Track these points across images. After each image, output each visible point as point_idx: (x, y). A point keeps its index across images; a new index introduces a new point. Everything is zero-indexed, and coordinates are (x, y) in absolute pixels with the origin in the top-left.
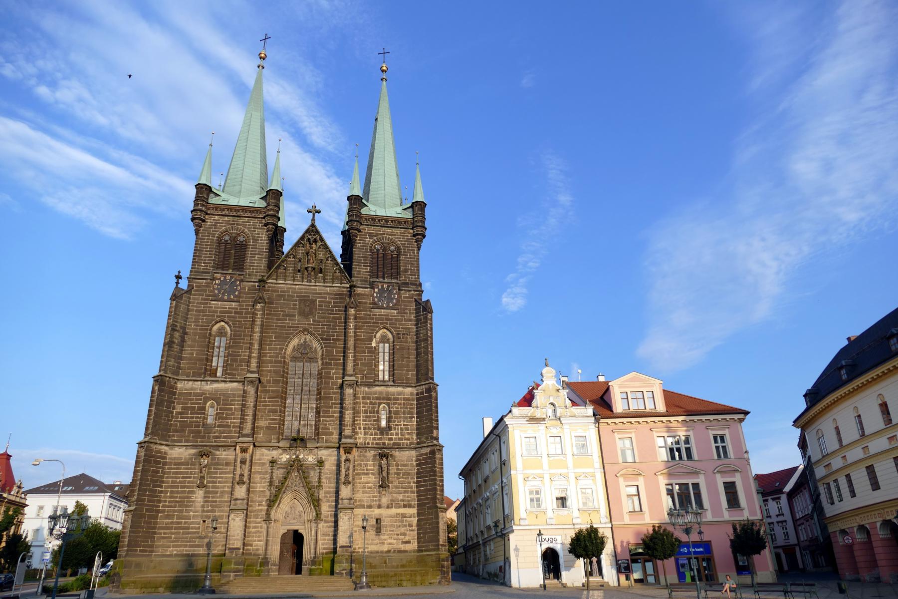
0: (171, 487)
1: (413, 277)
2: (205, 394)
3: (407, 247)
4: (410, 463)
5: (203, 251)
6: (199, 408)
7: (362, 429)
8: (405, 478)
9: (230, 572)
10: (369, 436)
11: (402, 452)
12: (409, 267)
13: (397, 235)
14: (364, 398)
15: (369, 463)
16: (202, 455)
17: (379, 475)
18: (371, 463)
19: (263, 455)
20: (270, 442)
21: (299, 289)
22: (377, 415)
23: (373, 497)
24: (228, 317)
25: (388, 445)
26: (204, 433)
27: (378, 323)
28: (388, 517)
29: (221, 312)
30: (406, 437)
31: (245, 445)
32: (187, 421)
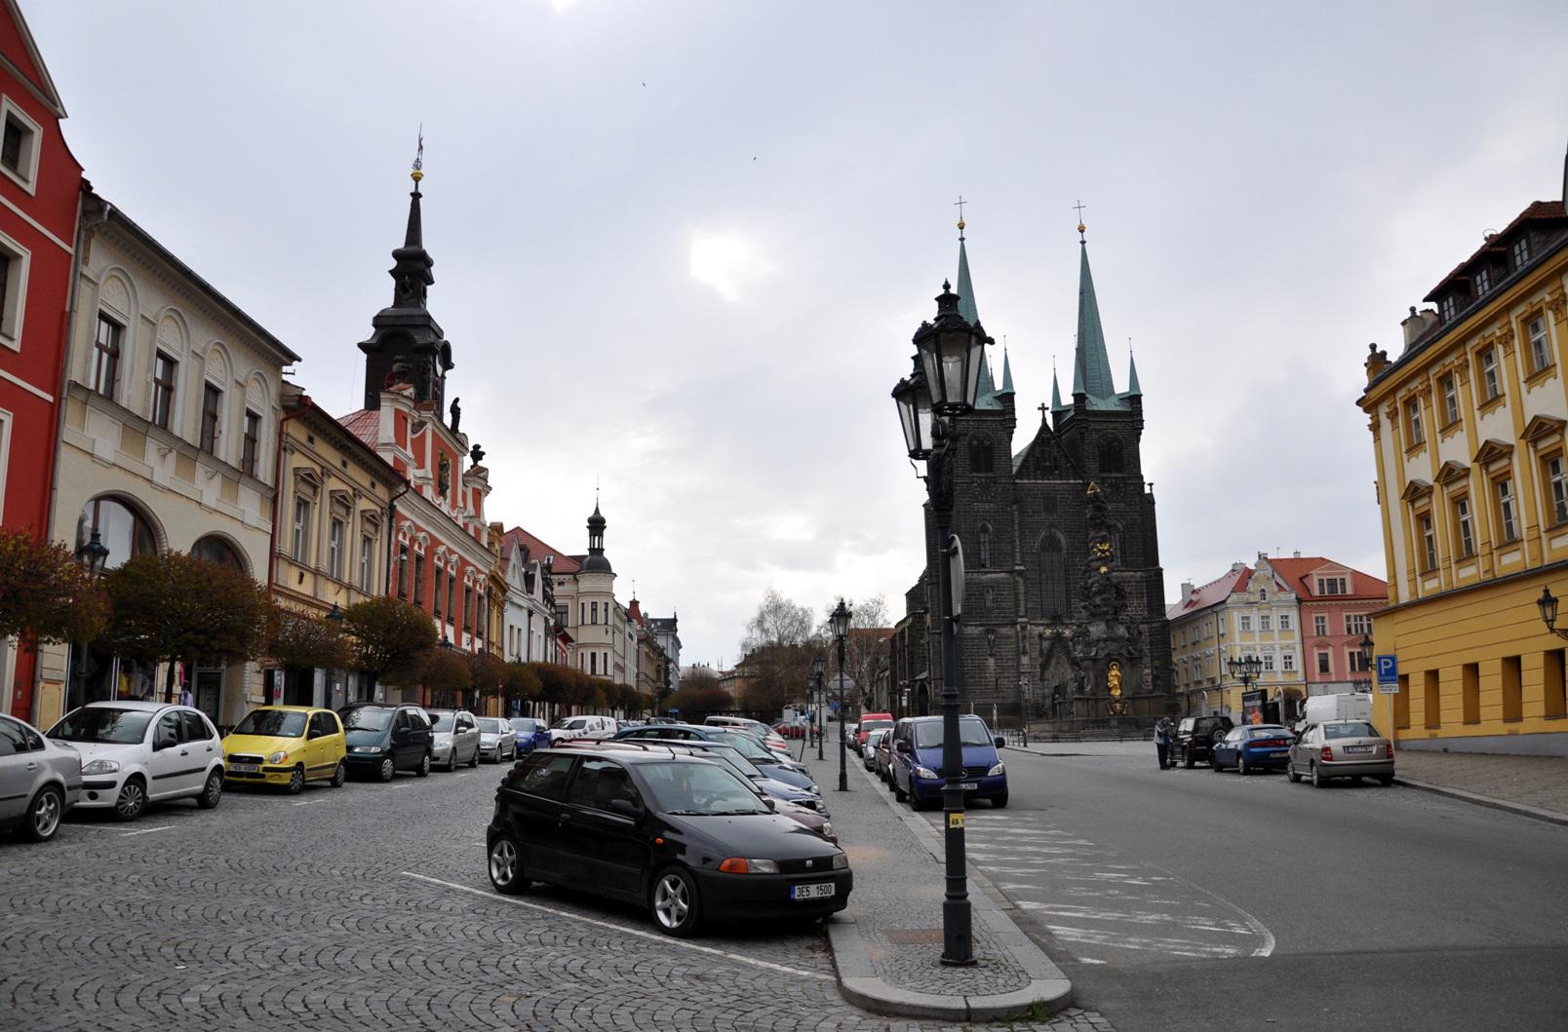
6: (980, 595)
16: (988, 632)
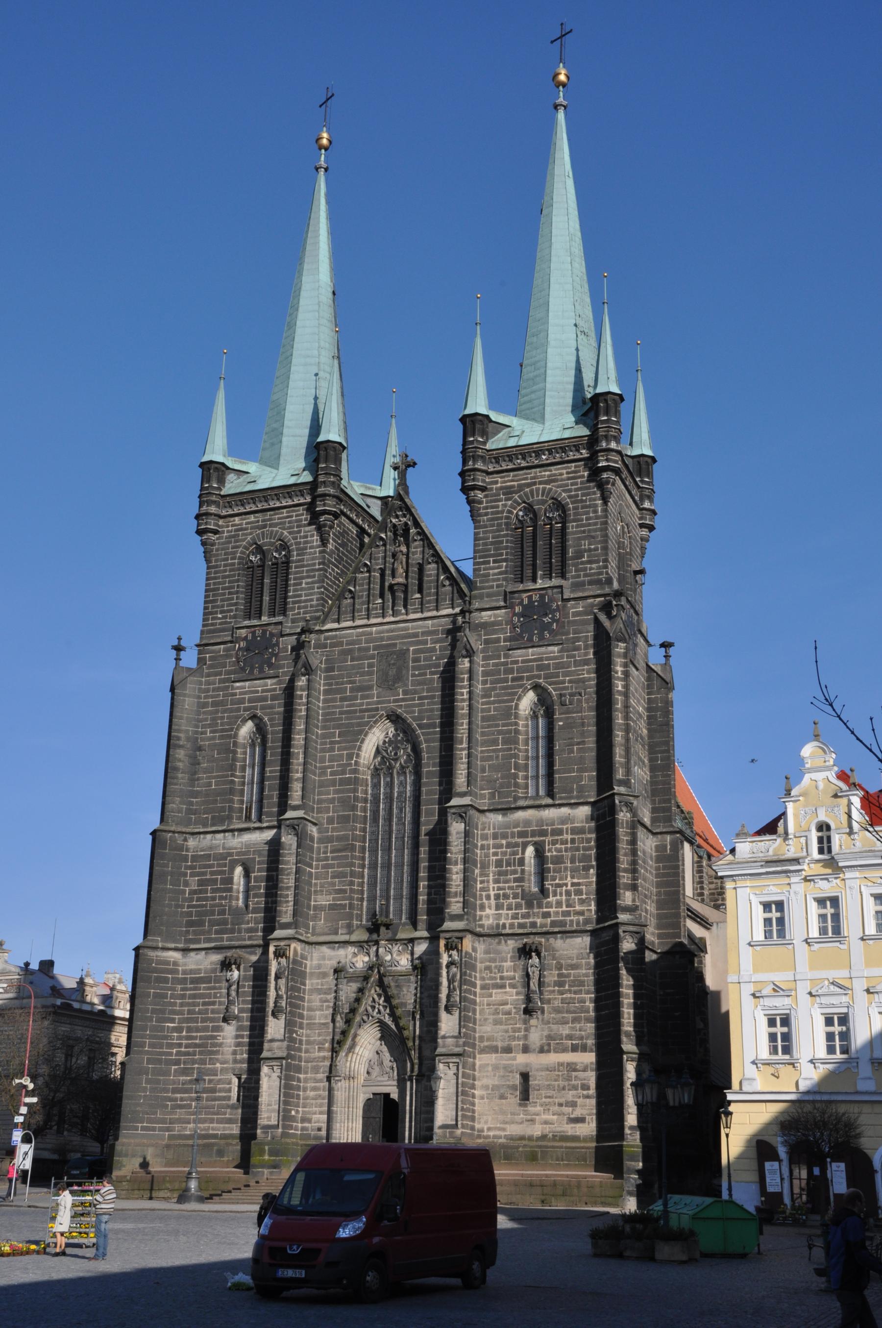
0: (188, 1020)
1: (594, 566)
2: (231, 854)
3: (582, 501)
4: (584, 961)
5: (218, 589)
7: (492, 897)
8: (575, 993)
9: (263, 1167)
10: (504, 912)
11: (568, 940)
12: (585, 544)
13: (562, 480)
14: (495, 837)
15: (505, 964)
17: (524, 987)
18: (509, 964)
19: (324, 958)
20: (336, 933)
21: (378, 632)
22: (519, 869)
23: (515, 1030)
24: (263, 708)
25: (542, 926)
26: (233, 924)
27: (521, 678)
28: (542, 1070)
29: (250, 700)
30: (578, 908)
31: (282, 943)
32: (205, 906)
